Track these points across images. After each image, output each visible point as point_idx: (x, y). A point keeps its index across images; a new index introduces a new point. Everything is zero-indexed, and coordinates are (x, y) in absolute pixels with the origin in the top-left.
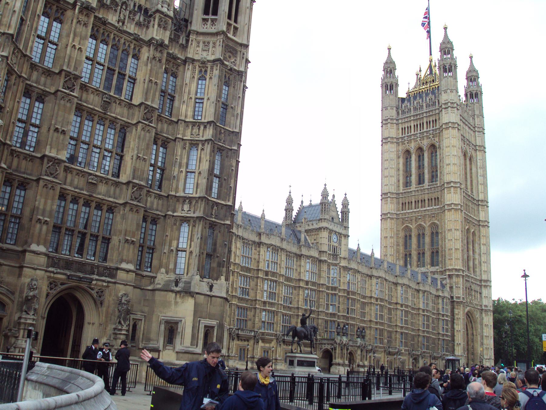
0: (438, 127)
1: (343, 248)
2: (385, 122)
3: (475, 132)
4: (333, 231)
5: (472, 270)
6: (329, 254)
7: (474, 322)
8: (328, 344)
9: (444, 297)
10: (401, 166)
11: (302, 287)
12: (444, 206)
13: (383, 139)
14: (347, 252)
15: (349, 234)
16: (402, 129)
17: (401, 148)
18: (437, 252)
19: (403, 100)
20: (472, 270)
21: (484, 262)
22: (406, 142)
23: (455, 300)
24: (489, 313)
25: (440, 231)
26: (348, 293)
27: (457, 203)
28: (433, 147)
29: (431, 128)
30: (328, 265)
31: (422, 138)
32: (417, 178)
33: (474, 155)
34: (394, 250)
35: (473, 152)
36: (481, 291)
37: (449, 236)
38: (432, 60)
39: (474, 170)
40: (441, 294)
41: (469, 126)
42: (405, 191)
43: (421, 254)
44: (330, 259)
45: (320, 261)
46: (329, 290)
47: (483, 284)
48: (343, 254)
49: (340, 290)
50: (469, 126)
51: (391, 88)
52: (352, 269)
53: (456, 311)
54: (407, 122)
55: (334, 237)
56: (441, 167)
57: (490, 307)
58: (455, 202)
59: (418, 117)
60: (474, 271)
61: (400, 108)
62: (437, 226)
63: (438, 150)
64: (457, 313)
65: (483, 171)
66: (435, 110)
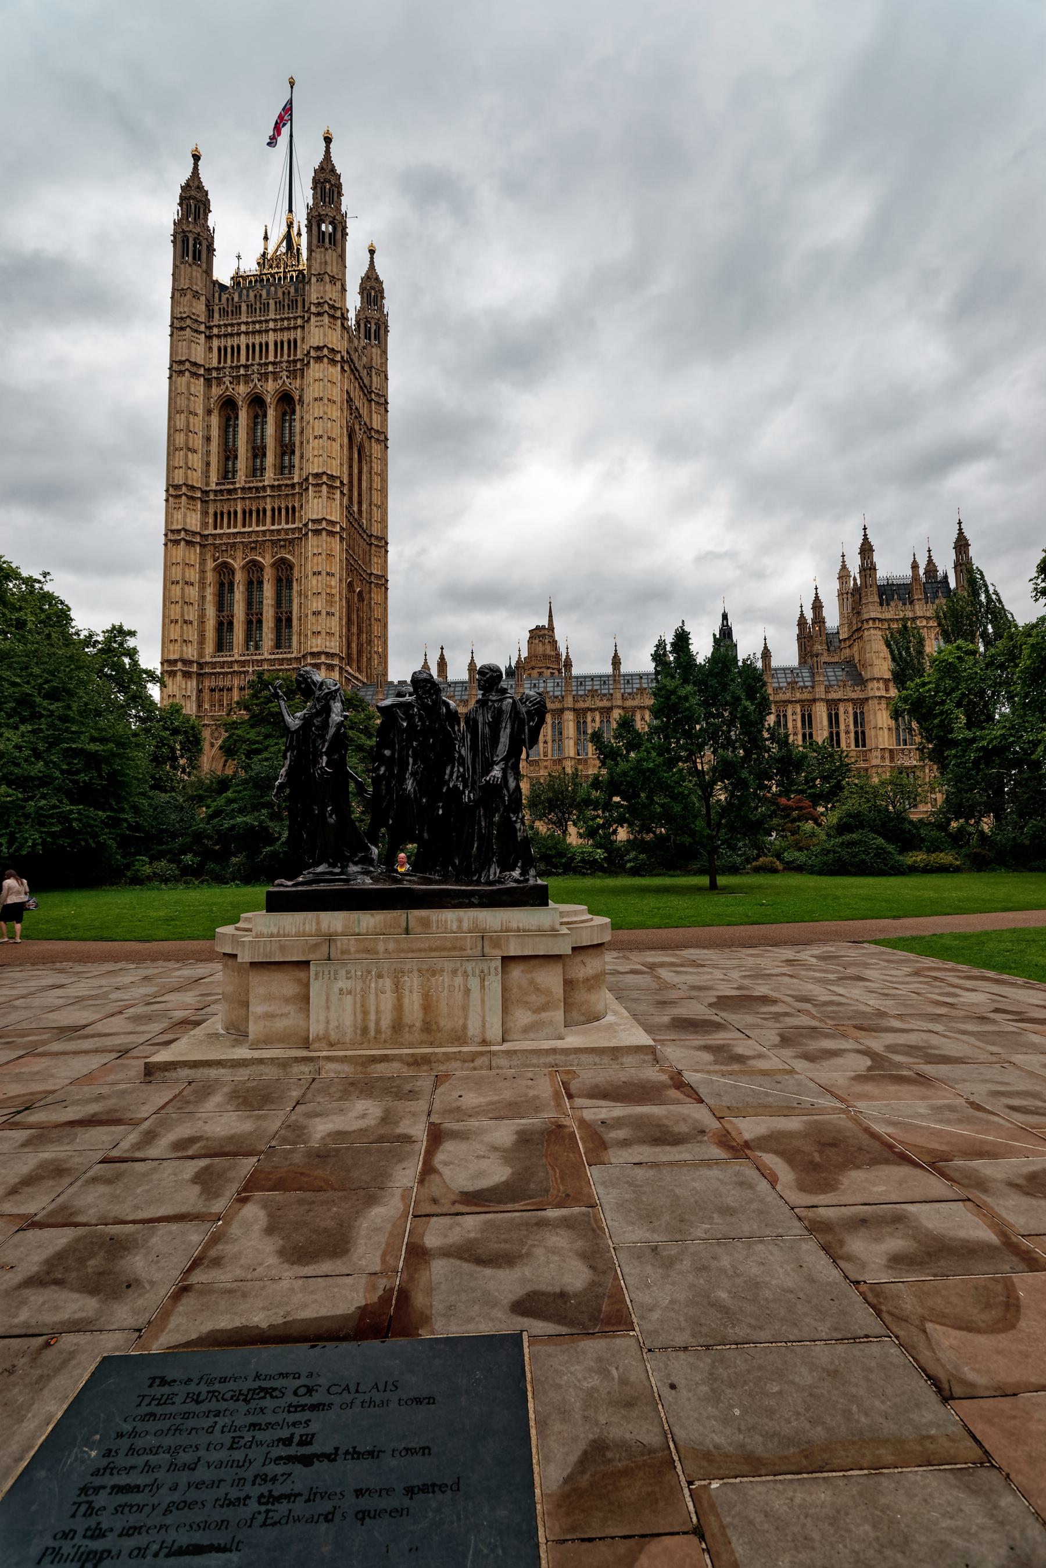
0: (298, 357)
2: (179, 325)
3: (370, 401)
10: (215, 433)
12: (306, 525)
13: (173, 362)
16: (219, 349)
17: (216, 391)
18: (289, 620)
19: (223, 288)
22: (227, 380)
25: (296, 574)
27: (333, 519)
28: (287, 401)
31: (264, 376)
33: (366, 444)
37: (314, 583)
38: (292, 223)
42: (223, 487)
43: (254, 624)
51: (197, 256)
54: (232, 335)
56: (302, 443)
58: (328, 517)
59: (257, 326)
61: (217, 301)
62: (290, 566)
63: (298, 408)
66: (295, 318)
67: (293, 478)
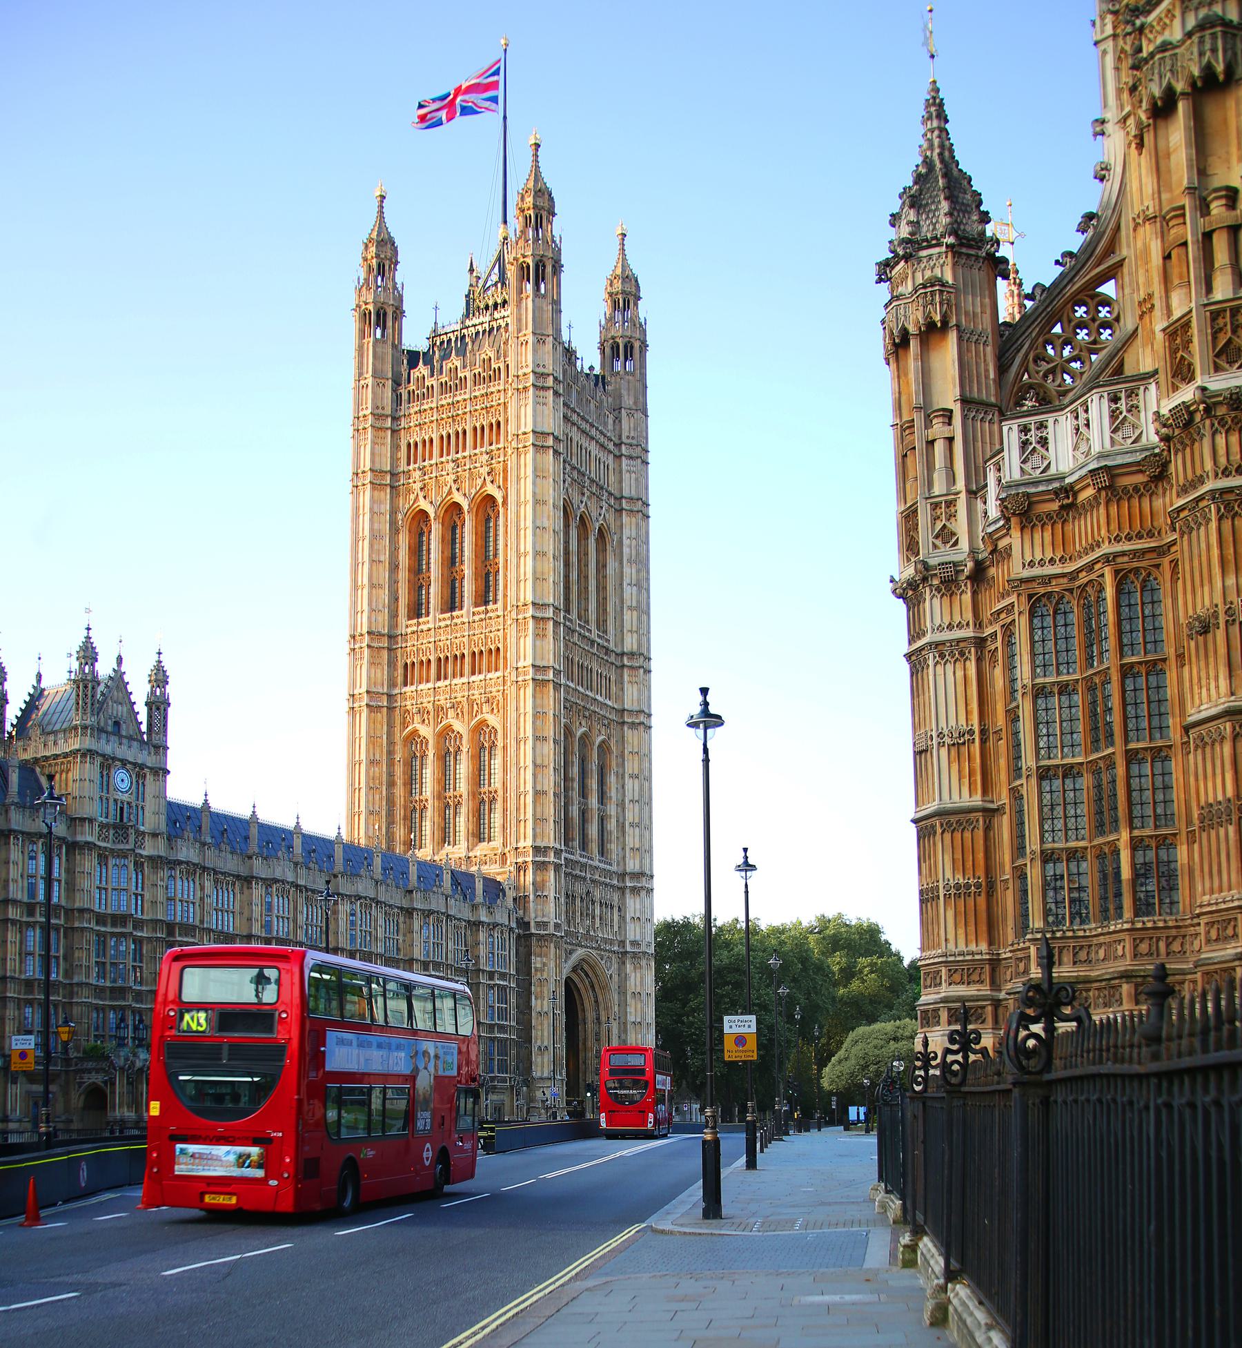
1: (150, 805)
3: (618, 457)
4: (114, 759)
5: (594, 847)
6: (102, 826)
7: (602, 988)
8: (97, 1071)
9: (495, 925)
11: (14, 922)
14: (163, 818)
15: (169, 768)
20: (594, 847)
21: (631, 825)
23: (533, 931)
24: (644, 962)
26: (170, 927)
29: (486, 448)
30: (100, 856)
32: (448, 592)
34: (381, 799)
35: (611, 517)
36: (624, 904)
39: (612, 565)
40: (483, 919)
41: (602, 439)
44: (106, 839)
45: (73, 847)
46: (105, 925)
47: (628, 884)
48: (151, 820)
49: (139, 924)
50: (602, 439)
52: (180, 863)
53: (536, 962)
55: (122, 779)
57: (649, 945)
60: (602, 852)
64: (538, 965)
65: (638, 571)
67: (497, 610)
